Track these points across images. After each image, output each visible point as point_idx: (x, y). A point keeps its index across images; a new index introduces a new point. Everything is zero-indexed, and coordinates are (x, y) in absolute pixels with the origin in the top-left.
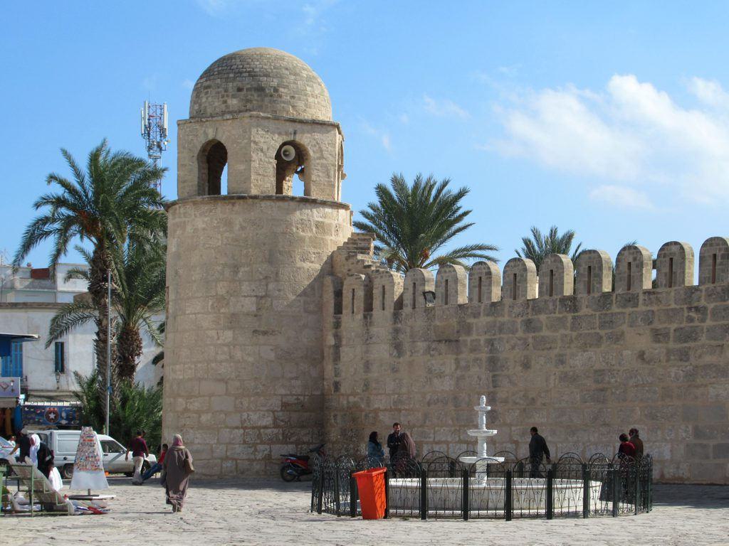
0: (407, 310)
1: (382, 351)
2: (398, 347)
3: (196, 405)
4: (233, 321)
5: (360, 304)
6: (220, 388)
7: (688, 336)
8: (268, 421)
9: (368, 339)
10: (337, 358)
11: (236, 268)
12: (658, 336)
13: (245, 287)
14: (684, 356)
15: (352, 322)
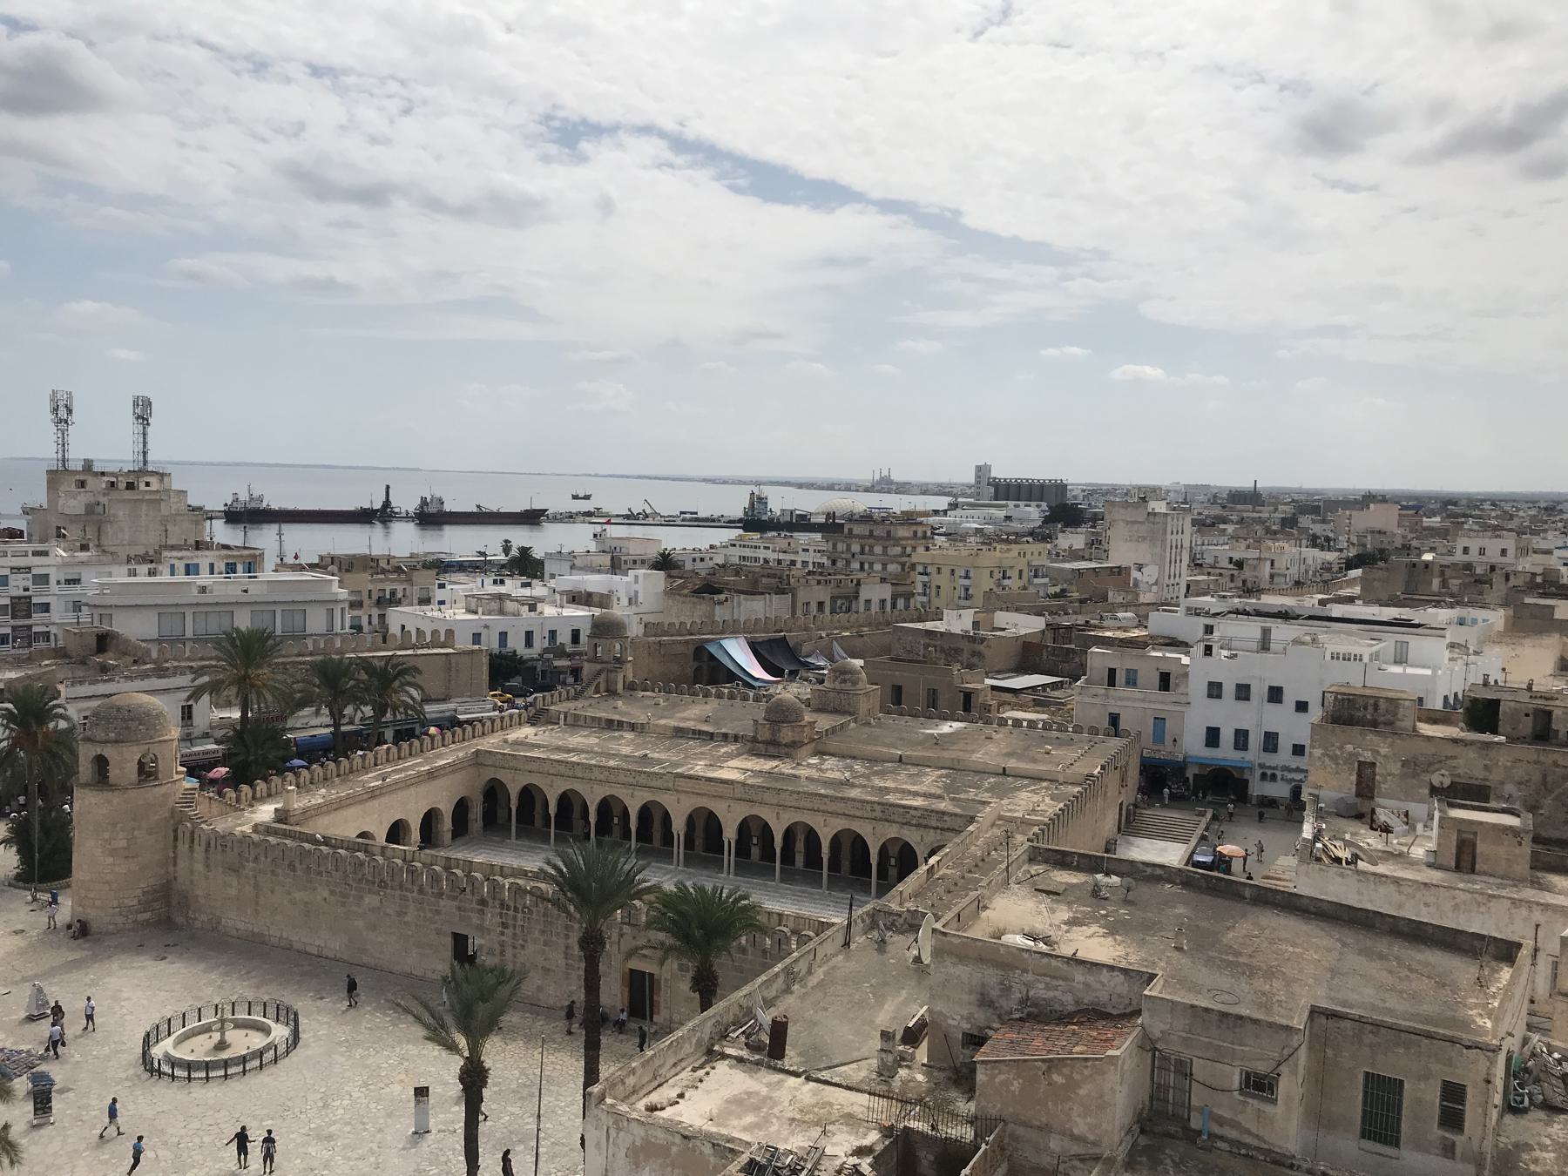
0: (212, 848)
1: (199, 867)
2: (207, 866)
3: (92, 895)
4: (114, 852)
5: (187, 840)
6: (106, 888)
7: (344, 896)
8: (135, 902)
9: (192, 858)
10: (175, 865)
11: (115, 825)
12: (332, 893)
13: (121, 835)
14: (343, 904)
15: (183, 847)
